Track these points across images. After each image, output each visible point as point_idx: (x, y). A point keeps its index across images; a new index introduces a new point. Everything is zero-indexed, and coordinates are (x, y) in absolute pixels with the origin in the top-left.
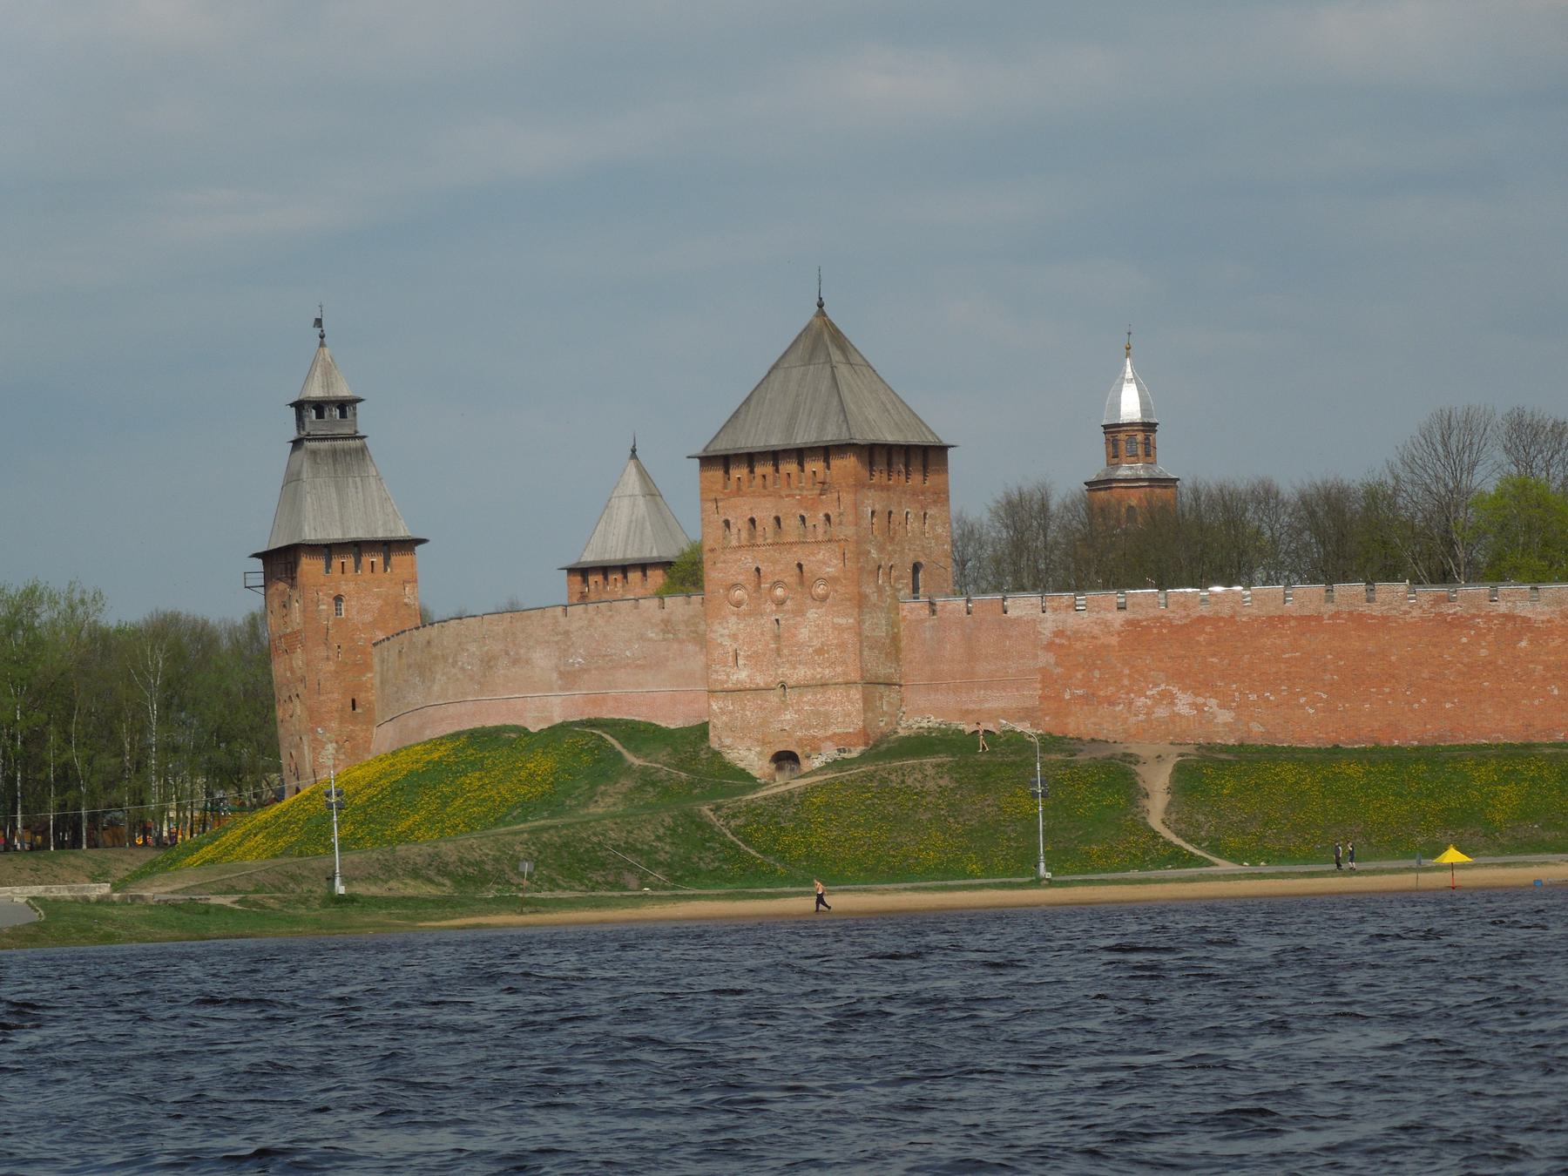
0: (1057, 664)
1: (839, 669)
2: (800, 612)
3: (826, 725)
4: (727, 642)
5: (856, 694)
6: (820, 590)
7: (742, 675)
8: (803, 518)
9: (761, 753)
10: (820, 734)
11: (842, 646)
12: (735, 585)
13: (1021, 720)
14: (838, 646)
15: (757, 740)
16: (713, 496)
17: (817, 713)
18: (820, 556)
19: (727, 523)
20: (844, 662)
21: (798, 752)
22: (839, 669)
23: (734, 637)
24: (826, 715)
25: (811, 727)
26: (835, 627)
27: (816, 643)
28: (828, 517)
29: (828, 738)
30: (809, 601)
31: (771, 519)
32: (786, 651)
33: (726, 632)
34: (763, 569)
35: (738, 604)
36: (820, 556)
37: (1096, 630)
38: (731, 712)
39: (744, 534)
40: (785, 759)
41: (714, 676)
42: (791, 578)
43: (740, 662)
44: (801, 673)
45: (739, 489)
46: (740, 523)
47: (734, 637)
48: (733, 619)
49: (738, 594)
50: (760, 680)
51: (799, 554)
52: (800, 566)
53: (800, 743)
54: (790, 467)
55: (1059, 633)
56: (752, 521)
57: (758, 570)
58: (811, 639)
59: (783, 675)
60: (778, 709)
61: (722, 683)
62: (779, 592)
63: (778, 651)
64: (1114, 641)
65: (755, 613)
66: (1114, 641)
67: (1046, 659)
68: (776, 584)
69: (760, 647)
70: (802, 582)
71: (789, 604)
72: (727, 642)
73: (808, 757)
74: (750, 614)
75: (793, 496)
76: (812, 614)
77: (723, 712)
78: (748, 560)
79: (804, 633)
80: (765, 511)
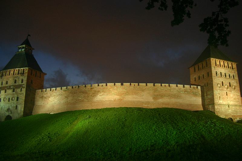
1: (238, 103)
4: (218, 95)
14: (238, 99)
18: (233, 82)
20: (239, 102)
21: (232, 118)
22: (238, 103)
23: (219, 94)
32: (229, 98)
34: (223, 82)
36: (233, 82)
42: (229, 85)
47: (219, 94)
48: (219, 90)
49: (219, 85)
53: (232, 116)
57: (222, 82)
63: (227, 98)
70: (230, 86)
72: (218, 95)
73: (234, 119)
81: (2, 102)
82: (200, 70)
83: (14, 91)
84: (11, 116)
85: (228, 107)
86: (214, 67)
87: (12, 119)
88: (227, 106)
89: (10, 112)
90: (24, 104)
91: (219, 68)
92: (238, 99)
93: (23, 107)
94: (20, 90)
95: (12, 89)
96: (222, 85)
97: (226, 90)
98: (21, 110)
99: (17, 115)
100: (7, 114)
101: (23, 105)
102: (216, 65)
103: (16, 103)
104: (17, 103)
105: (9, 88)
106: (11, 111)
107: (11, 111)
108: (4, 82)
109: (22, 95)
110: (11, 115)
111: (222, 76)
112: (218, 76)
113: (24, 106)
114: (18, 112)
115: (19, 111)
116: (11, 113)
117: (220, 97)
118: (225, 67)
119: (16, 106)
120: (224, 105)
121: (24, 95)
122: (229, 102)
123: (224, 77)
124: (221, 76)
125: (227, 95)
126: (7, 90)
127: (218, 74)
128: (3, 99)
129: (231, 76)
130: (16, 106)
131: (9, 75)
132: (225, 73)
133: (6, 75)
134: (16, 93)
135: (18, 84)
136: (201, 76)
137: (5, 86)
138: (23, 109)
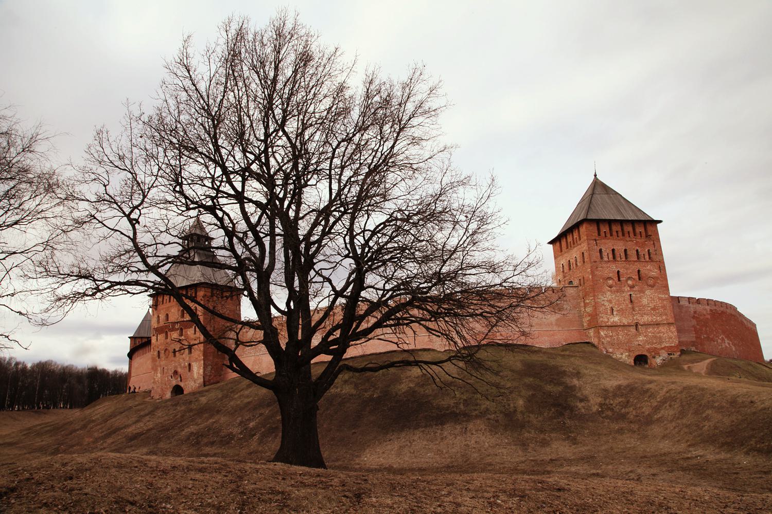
0: (697, 325)
1: (664, 317)
2: (642, 291)
3: (661, 343)
4: (606, 304)
5: (673, 329)
6: (651, 282)
7: (616, 319)
8: (637, 251)
9: (629, 356)
10: (658, 346)
11: (664, 307)
12: (610, 278)
13: (692, 346)
14: (662, 307)
15: (626, 349)
16: (594, 238)
17: (656, 337)
18: (648, 268)
19: (601, 251)
20: (666, 315)
22: (664, 317)
23: (610, 301)
24: (660, 338)
25: (653, 343)
26: (660, 299)
27: (652, 305)
28: (649, 251)
29: (662, 349)
30: (646, 287)
31: (623, 250)
33: (606, 299)
35: (611, 287)
36: (648, 268)
37: (705, 313)
38: (612, 336)
39: (611, 256)
40: (641, 360)
41: (601, 319)
42: (637, 277)
43: (615, 313)
44: (646, 319)
45: (606, 236)
46: (607, 252)
47: (610, 301)
49: (610, 282)
50: (625, 321)
51: (637, 266)
52: (639, 271)
53: (648, 350)
54: (629, 228)
55: (695, 312)
56: (613, 250)
57: (618, 272)
58: (648, 304)
59: (637, 319)
60: (636, 335)
61: (606, 322)
62: (630, 282)
63: (633, 309)
64: (709, 317)
65: (619, 291)
66: (709, 317)
67: (694, 322)
68: (629, 278)
69: (623, 306)
71: (636, 288)
72: (606, 304)
73: (654, 357)
74: (617, 291)
75: (633, 241)
76: (648, 292)
77: (607, 336)
78: (614, 267)
79: (645, 301)
80: (620, 247)
82: (569, 247)
83: (181, 335)
84: (182, 386)
85: (635, 330)
86: (596, 240)
87: (185, 393)
88: (635, 327)
89: (179, 379)
90: (204, 360)
91: (607, 241)
92: (662, 307)
94: (193, 332)
95: (178, 329)
96: (616, 279)
97: (628, 291)
98: (199, 373)
101: (202, 362)
102: (599, 234)
103: (187, 359)
104: (190, 358)
106: (181, 377)
107: (181, 377)
108: (162, 317)
110: (182, 384)
111: (619, 259)
112: (606, 259)
113: (204, 364)
114: (193, 376)
115: (195, 376)
116: (181, 381)
117: (613, 310)
118: (627, 235)
119: (190, 365)
120: (624, 326)
122: (637, 317)
123: (624, 259)
124: (614, 257)
125: (631, 302)
126: (169, 333)
127: (605, 254)
129: (641, 253)
130: (190, 365)
131: (170, 302)
132: (625, 250)
133: (165, 302)
134: (187, 336)
136: (572, 261)
138: (201, 371)
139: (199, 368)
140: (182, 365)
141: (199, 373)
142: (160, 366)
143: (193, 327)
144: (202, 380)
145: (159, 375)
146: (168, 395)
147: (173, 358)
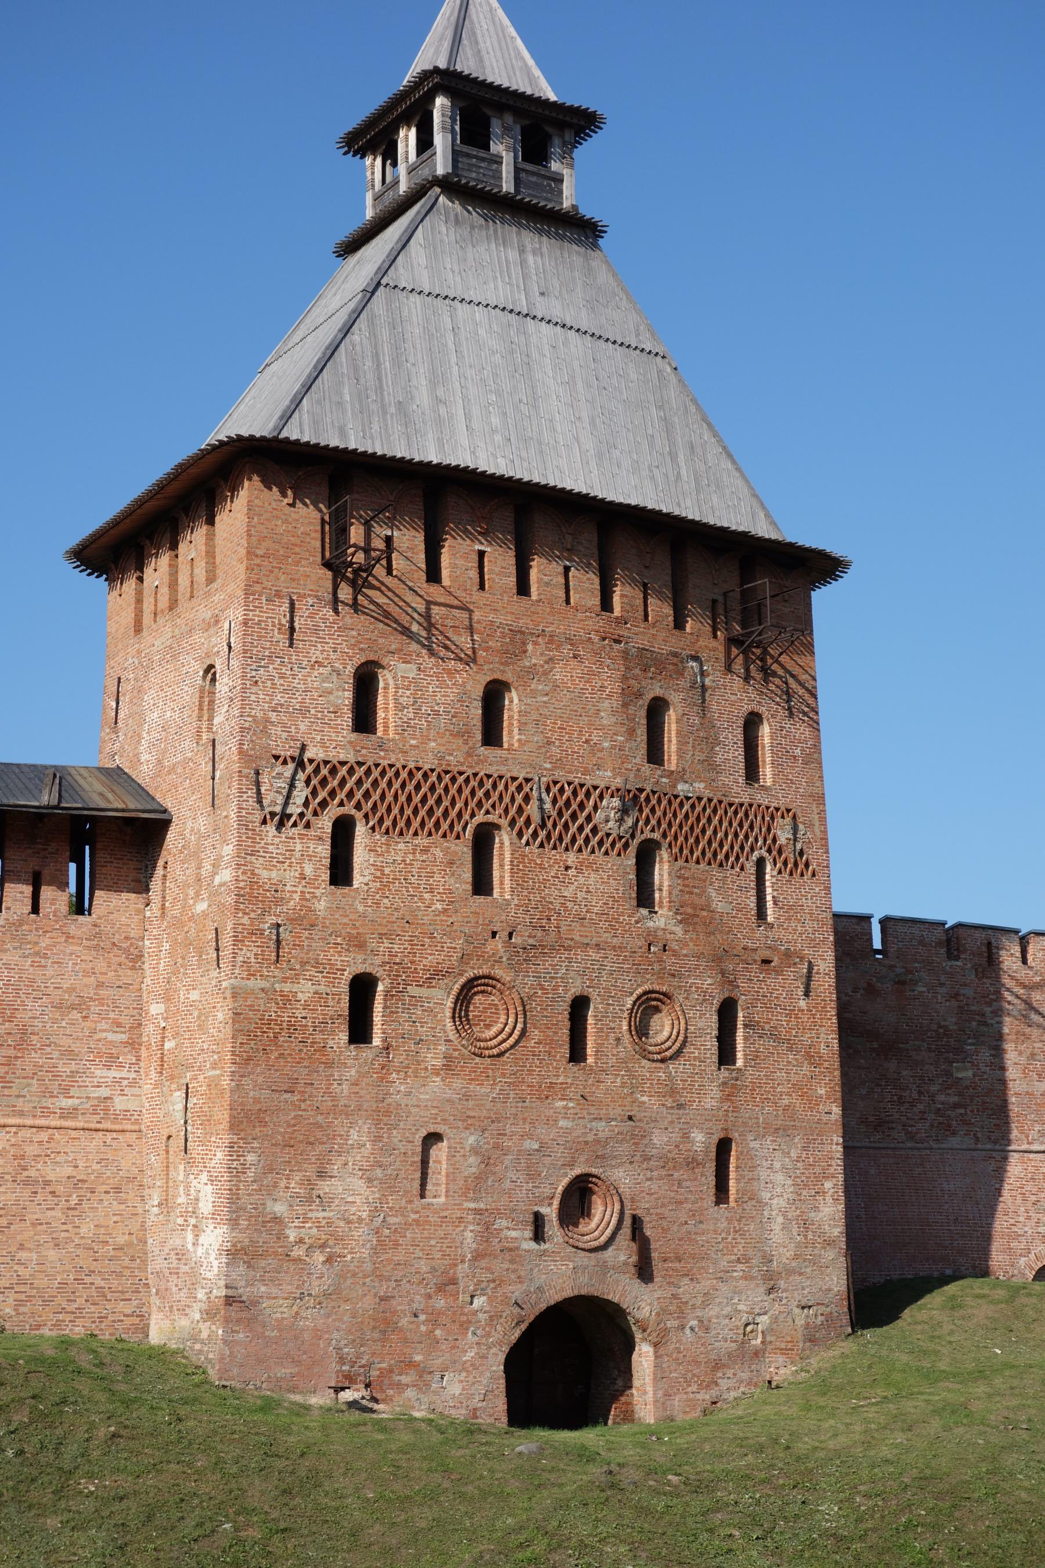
81: (433, 1059)
89: (623, 1253)
93: (837, 1166)
98: (805, 1224)
99: (756, 1294)
100: (558, 1273)
101: (835, 1146)
103: (711, 1099)
105: (564, 819)
109: (791, 979)
110: (640, 1302)
115: (780, 1240)
121: (826, 982)
128: (442, 999)
135: (700, 786)
137: (455, 760)
138: (830, 1213)
139: (807, 1185)
140: (659, 1139)
141: (805, 1224)
142: (383, 1116)
143: (751, 868)
144: (835, 1280)
145: (351, 1191)
146: (469, 1382)
147: (566, 1074)
